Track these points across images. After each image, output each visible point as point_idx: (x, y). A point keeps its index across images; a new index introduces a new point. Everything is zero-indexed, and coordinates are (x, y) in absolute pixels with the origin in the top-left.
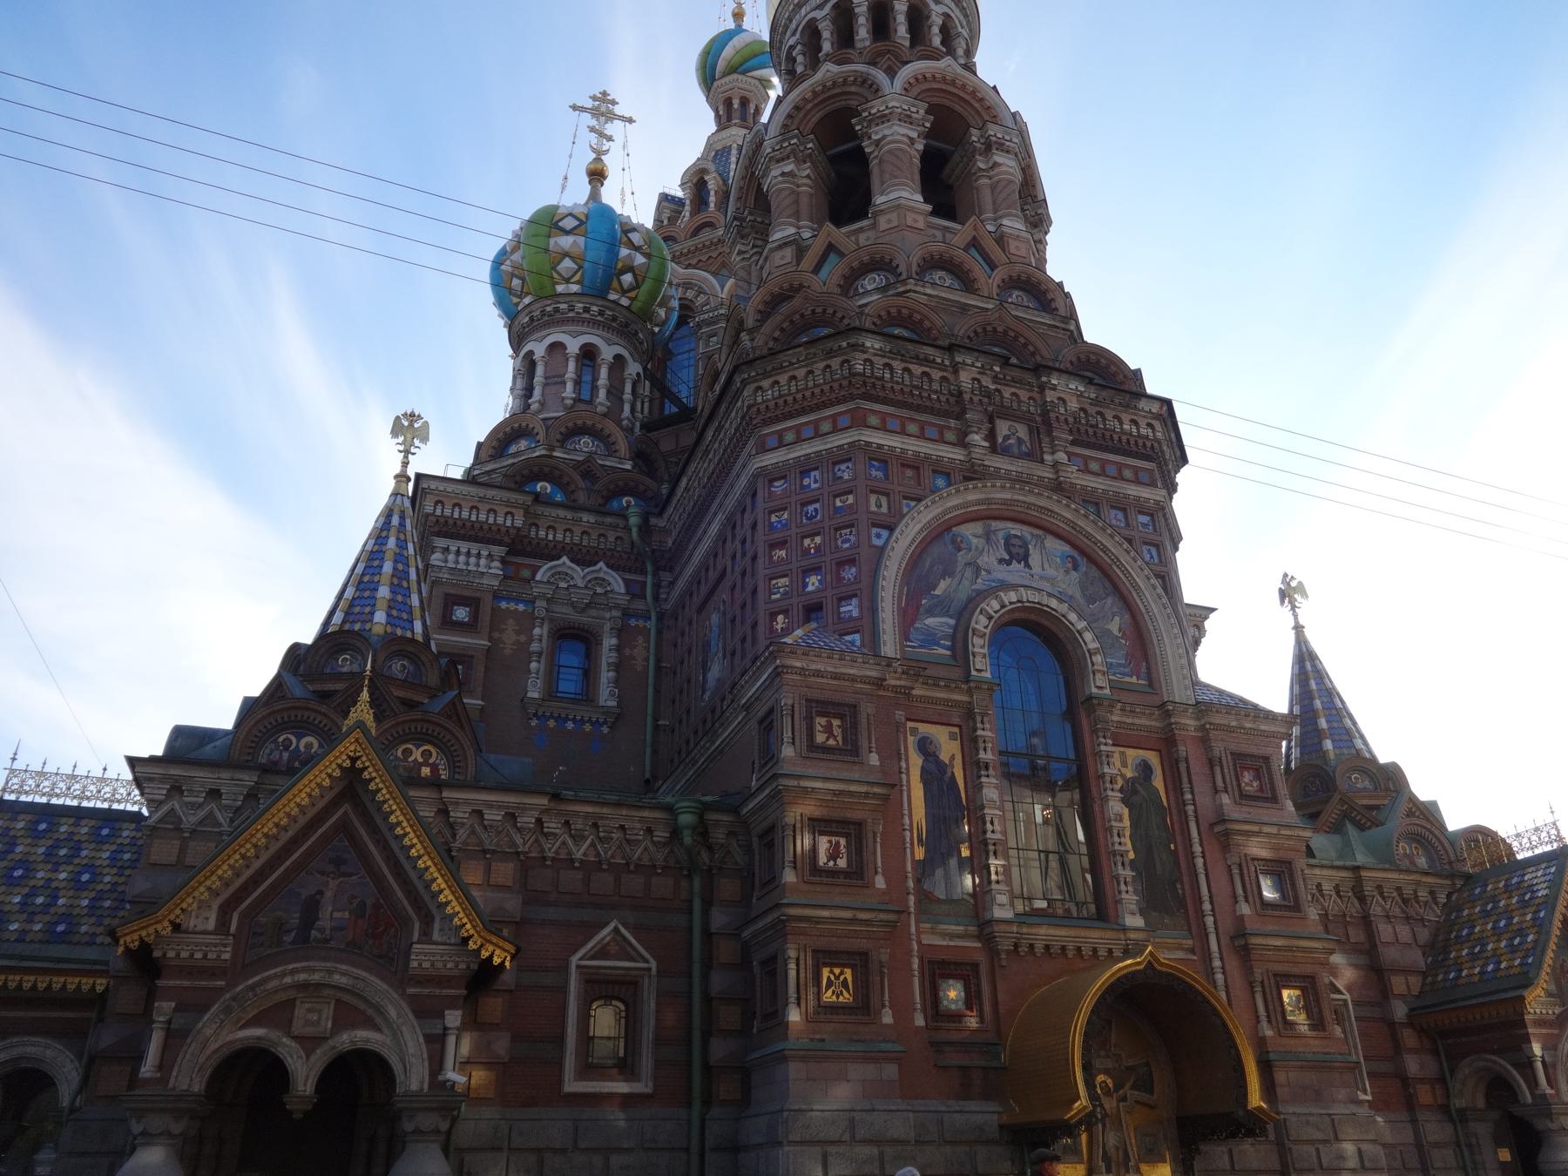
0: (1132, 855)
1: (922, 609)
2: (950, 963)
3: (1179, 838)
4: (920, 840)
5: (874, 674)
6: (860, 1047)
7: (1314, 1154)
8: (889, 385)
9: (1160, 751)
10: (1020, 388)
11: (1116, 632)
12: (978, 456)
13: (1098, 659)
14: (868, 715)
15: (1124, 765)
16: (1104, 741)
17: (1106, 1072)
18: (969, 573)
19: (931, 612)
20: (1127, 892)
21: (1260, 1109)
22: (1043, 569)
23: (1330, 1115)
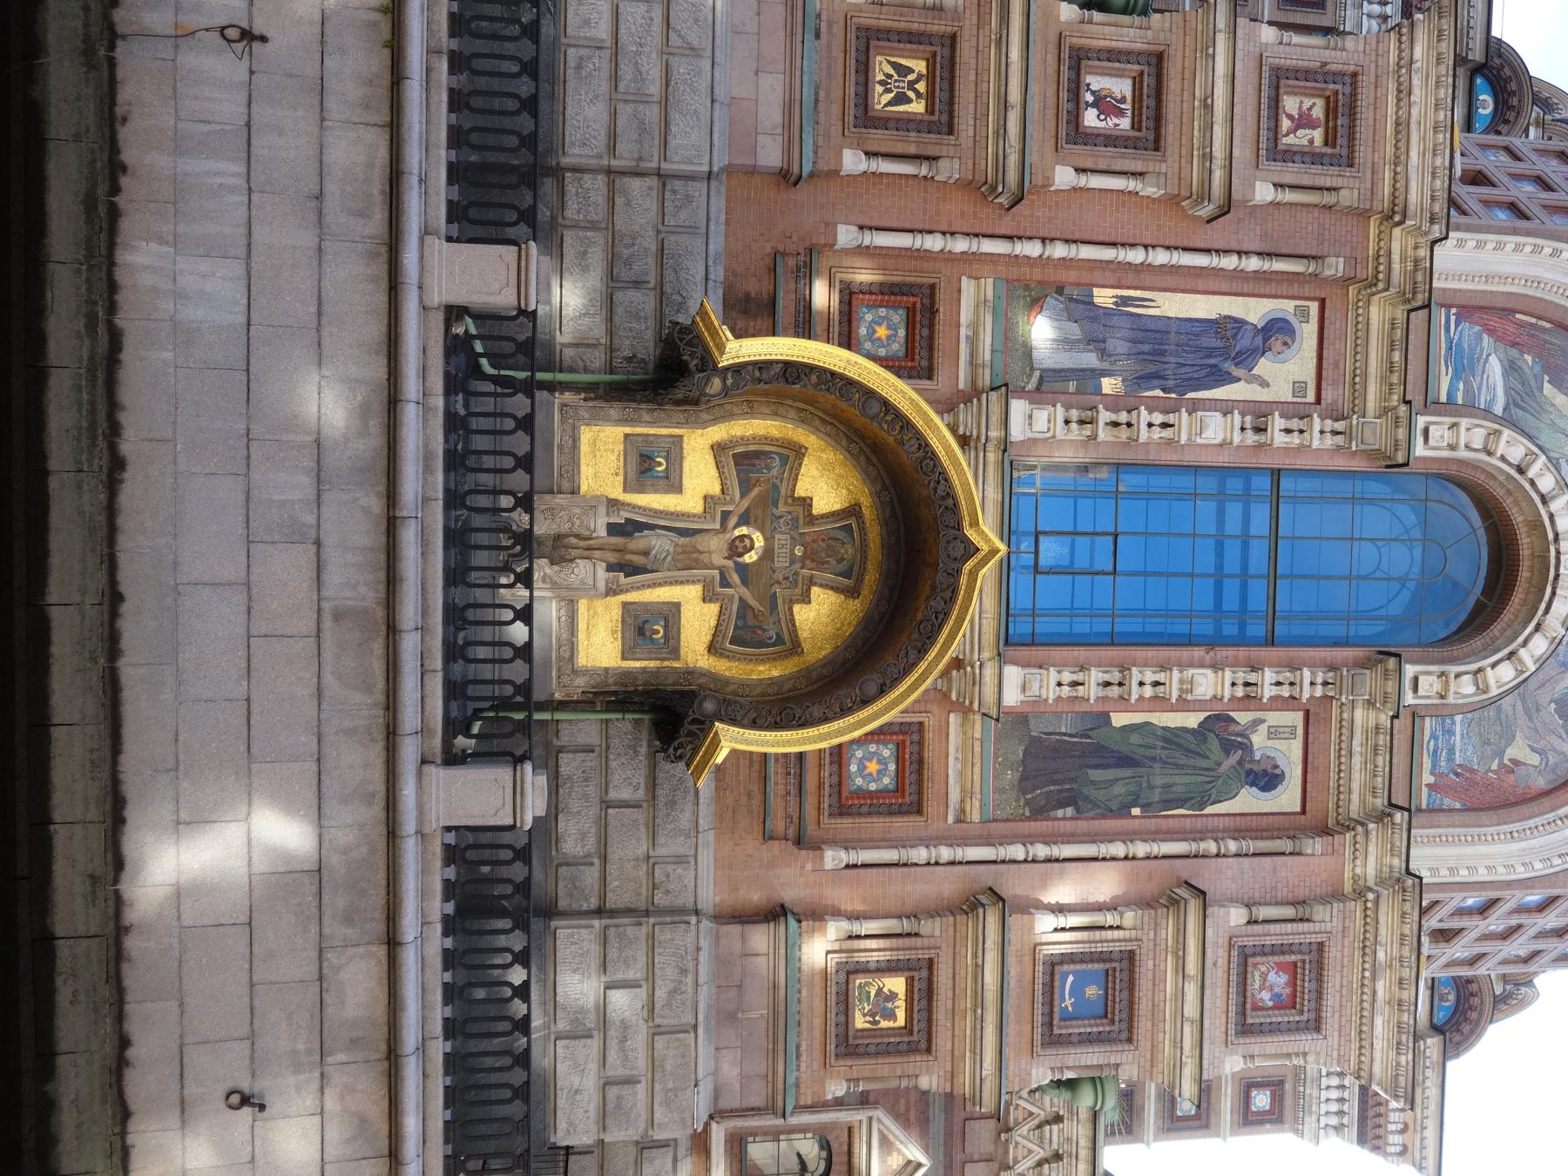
0: (1119, 720)
1: (1514, 352)
2: (931, 326)
3: (1152, 824)
4: (1125, 301)
5: (1413, 197)
6: (808, 94)
7: (630, 975)
9: (1304, 811)
11: (1512, 752)
13: (1467, 687)
15: (1273, 733)
16: (1319, 680)
17: (768, 554)
19: (1511, 368)
21: (716, 744)
23: (695, 1027)
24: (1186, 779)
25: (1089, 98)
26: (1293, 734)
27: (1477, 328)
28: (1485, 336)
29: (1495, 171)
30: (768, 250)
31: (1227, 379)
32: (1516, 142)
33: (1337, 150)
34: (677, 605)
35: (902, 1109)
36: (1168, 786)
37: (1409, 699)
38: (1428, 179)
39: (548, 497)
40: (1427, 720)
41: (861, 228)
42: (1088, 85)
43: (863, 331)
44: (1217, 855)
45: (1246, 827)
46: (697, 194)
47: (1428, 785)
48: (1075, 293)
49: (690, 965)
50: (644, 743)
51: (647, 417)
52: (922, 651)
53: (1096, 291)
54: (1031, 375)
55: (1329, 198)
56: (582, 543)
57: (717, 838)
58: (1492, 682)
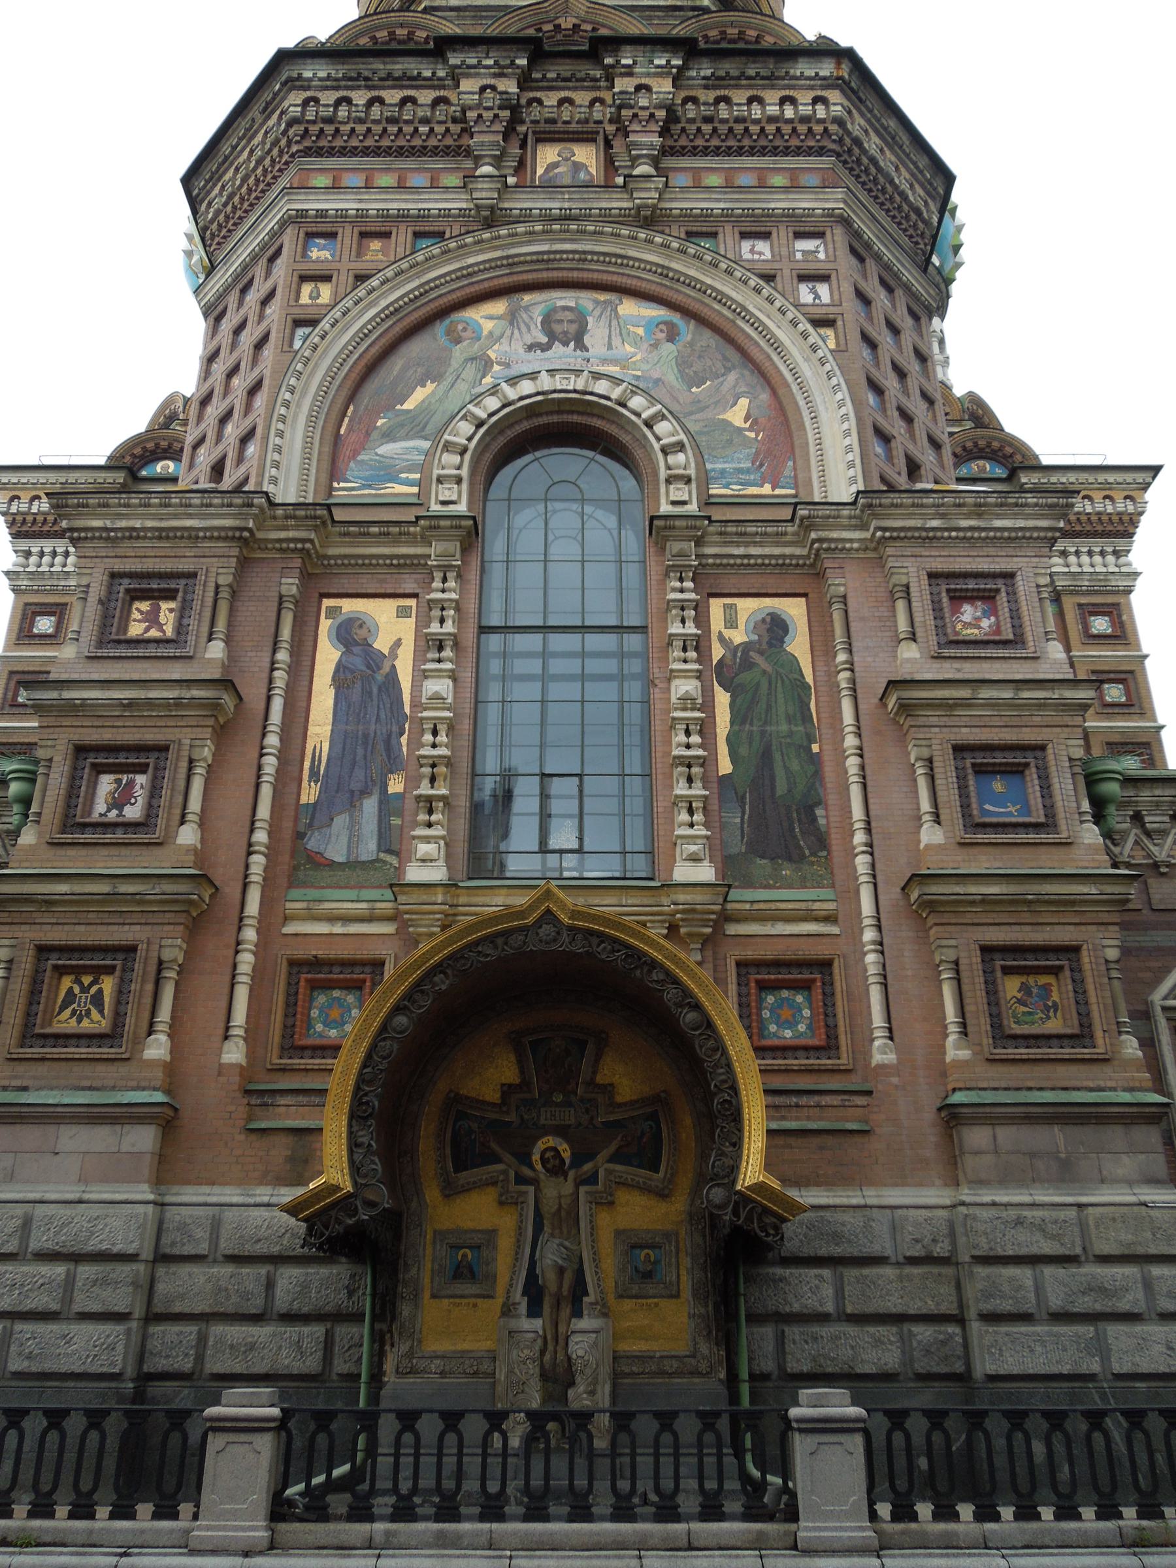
0: (725, 766)
1: (375, 435)
4: (314, 774)
8: (348, 128)
9: (805, 595)
10: (575, 89)
12: (484, 195)
14: (217, 587)
15: (731, 623)
16: (678, 584)
17: (561, 1131)
18: (470, 372)
19: (389, 436)
20: (692, 825)
21: (760, 1187)
22: (610, 347)
23: (1080, 1206)
24: (781, 701)
25: (114, 812)
26: (732, 607)
27: (352, 464)
28: (359, 458)
29: (213, 456)
30: (242, 1137)
31: (392, 678)
32: (190, 439)
33: (181, 588)
34: (618, 1233)
35: (1148, 975)
36: (790, 719)
37: (693, 508)
38: (212, 510)
39: (500, 1389)
40: (711, 492)
41: (226, 1038)
42: (101, 815)
43: (333, 1033)
44: (852, 671)
45: (822, 645)
46: (178, 1218)
47: (773, 489)
48: (305, 821)
49: (1013, 1213)
50: (771, 1270)
51: (414, 1271)
52: (654, 964)
53: (304, 799)
54: (385, 862)
55: (225, 594)
56: (550, 1347)
57: (872, 1183)
58: (673, 439)
